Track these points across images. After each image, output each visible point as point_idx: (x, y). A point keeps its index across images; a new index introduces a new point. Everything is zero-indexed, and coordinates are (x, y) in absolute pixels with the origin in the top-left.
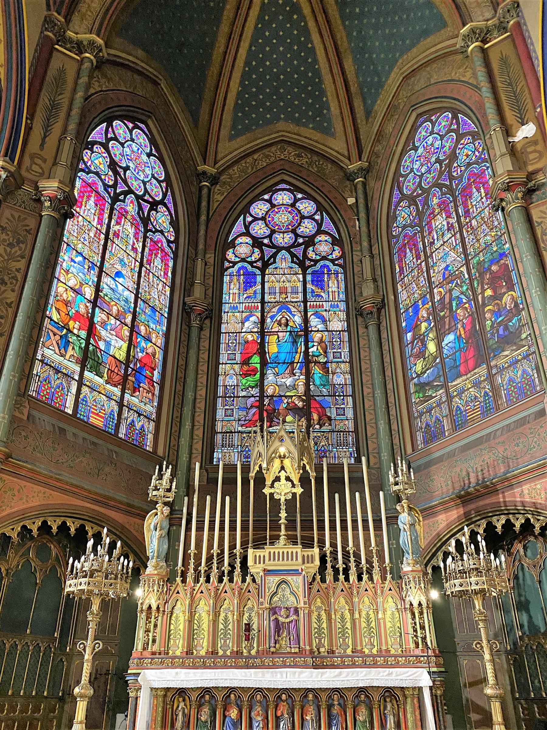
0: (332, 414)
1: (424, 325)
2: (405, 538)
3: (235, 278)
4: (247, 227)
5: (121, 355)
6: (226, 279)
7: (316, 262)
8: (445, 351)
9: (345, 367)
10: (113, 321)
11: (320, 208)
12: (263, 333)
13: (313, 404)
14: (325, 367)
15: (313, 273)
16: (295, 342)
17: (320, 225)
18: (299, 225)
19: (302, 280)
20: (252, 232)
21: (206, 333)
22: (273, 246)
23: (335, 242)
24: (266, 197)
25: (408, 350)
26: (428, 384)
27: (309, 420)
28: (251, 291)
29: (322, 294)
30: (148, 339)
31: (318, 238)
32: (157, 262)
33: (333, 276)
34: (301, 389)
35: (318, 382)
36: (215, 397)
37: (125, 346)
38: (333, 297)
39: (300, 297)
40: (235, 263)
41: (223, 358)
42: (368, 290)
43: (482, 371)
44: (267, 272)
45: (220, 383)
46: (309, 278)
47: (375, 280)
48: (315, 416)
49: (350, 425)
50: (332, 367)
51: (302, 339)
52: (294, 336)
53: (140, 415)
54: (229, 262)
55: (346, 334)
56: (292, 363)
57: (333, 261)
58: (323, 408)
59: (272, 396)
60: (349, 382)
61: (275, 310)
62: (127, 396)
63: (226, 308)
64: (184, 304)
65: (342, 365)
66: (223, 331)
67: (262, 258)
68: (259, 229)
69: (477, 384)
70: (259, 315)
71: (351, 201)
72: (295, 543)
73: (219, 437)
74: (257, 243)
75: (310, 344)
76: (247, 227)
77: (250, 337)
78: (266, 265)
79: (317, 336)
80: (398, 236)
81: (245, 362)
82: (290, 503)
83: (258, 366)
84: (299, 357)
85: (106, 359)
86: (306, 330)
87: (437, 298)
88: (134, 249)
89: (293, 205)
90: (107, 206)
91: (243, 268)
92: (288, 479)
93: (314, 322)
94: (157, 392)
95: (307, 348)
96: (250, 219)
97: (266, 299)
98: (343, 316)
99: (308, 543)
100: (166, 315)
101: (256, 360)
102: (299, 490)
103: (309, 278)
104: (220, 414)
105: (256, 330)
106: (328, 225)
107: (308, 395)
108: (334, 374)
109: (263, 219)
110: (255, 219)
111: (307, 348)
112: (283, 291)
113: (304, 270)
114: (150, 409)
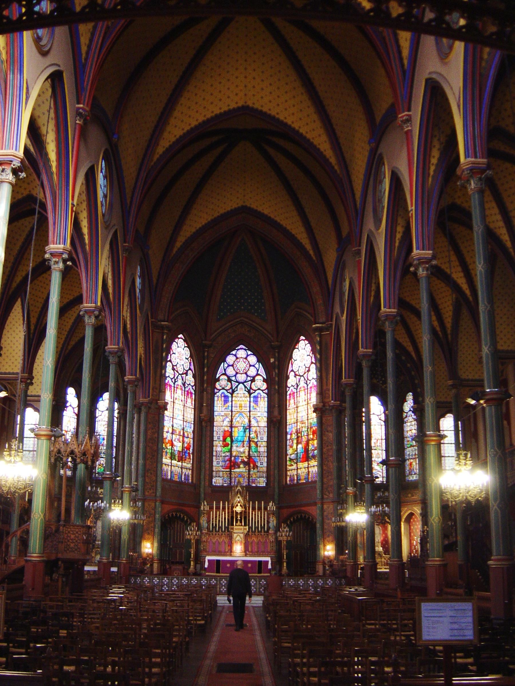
0: (259, 464)
1: (294, 435)
2: (271, 525)
3: (220, 398)
4: (225, 370)
5: (180, 449)
6: (216, 398)
7: (255, 391)
8: (298, 450)
9: (265, 444)
10: (178, 437)
11: (258, 361)
12: (231, 427)
13: (251, 460)
14: (256, 443)
15: (254, 397)
16: (245, 432)
17: (258, 371)
18: (249, 370)
19: (249, 400)
20: (227, 373)
21: (209, 428)
22: (237, 382)
23: (264, 380)
24: (234, 352)
25: (288, 442)
26: (293, 460)
27: (249, 466)
28: (227, 405)
29: (257, 408)
30: (188, 437)
31: (257, 378)
32: (189, 400)
33: (262, 399)
34: (247, 454)
35: (253, 450)
36: (213, 456)
37: (181, 444)
38: (262, 410)
39: (248, 408)
40: (220, 390)
41: (215, 438)
42: (276, 413)
43: (306, 464)
44: (234, 396)
45: (214, 449)
46: (252, 399)
47: (279, 406)
48: (252, 465)
49: (265, 469)
50: (259, 444)
51: (248, 430)
52: (245, 429)
53: (187, 469)
54: (217, 389)
55: (266, 428)
56: (243, 441)
57: (262, 391)
58: (255, 462)
59: (235, 456)
60: (266, 451)
61: (237, 415)
62: (183, 464)
63: (216, 413)
64: (200, 417)
65: (264, 443)
66: (215, 425)
67: (231, 388)
68: (230, 371)
69: (305, 468)
70: (230, 418)
71: (272, 360)
72: (242, 525)
73: (214, 473)
74: (229, 380)
75: (251, 433)
76: (225, 370)
77: (226, 429)
78: (233, 391)
79: (253, 429)
80: (289, 388)
81: (224, 440)
82: (241, 513)
83: (230, 443)
84: (247, 439)
85: (176, 453)
86: (250, 426)
87: (298, 427)
88: (182, 401)
89: (246, 358)
90: (173, 388)
91: (223, 393)
92: (241, 506)
93: (253, 422)
94: (191, 458)
95: (250, 434)
96: (226, 365)
97: (233, 410)
98: (266, 419)
99: (245, 525)
100: (193, 423)
101: (228, 440)
102: (244, 509)
103: (252, 399)
104: (215, 463)
105: (229, 425)
106: (262, 371)
107: (249, 457)
108: (260, 447)
109: (232, 366)
110: (229, 366)
111: (250, 434)
112: (241, 406)
113: (250, 394)
114: (189, 466)
